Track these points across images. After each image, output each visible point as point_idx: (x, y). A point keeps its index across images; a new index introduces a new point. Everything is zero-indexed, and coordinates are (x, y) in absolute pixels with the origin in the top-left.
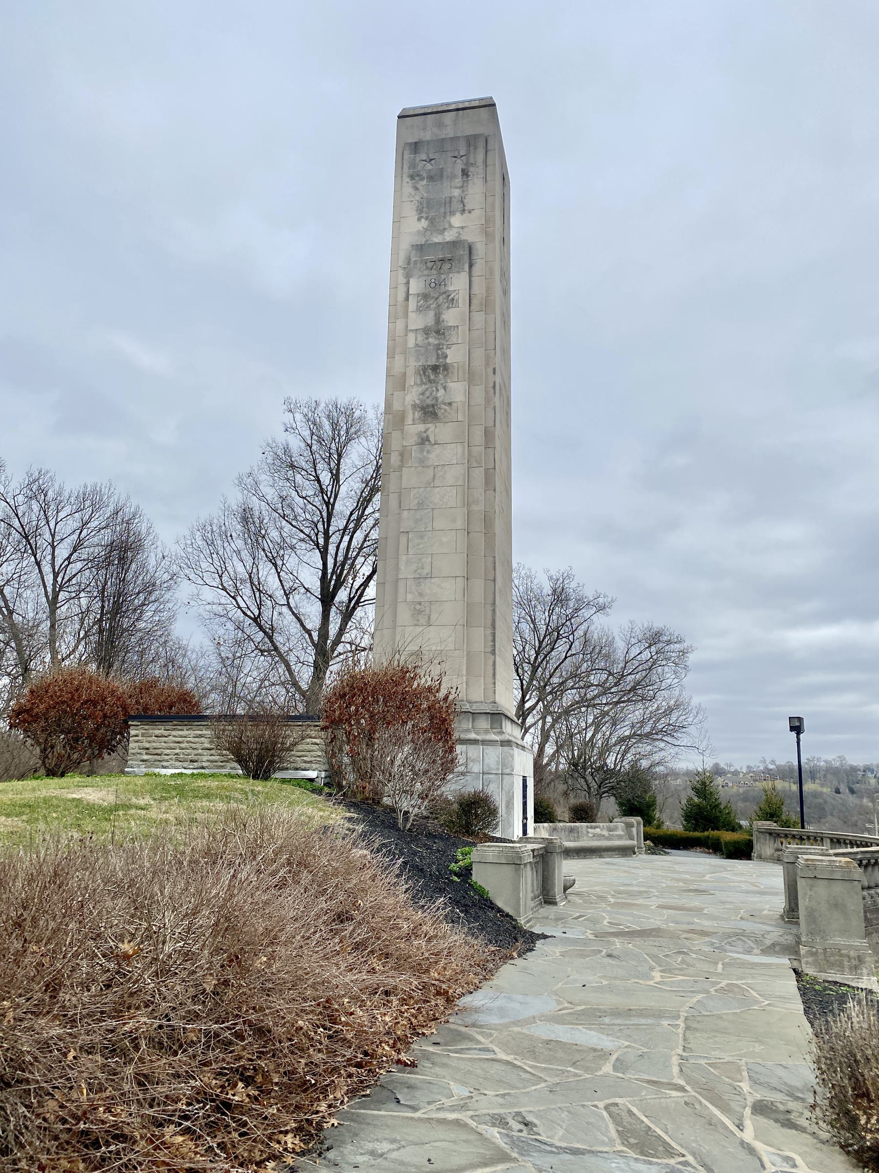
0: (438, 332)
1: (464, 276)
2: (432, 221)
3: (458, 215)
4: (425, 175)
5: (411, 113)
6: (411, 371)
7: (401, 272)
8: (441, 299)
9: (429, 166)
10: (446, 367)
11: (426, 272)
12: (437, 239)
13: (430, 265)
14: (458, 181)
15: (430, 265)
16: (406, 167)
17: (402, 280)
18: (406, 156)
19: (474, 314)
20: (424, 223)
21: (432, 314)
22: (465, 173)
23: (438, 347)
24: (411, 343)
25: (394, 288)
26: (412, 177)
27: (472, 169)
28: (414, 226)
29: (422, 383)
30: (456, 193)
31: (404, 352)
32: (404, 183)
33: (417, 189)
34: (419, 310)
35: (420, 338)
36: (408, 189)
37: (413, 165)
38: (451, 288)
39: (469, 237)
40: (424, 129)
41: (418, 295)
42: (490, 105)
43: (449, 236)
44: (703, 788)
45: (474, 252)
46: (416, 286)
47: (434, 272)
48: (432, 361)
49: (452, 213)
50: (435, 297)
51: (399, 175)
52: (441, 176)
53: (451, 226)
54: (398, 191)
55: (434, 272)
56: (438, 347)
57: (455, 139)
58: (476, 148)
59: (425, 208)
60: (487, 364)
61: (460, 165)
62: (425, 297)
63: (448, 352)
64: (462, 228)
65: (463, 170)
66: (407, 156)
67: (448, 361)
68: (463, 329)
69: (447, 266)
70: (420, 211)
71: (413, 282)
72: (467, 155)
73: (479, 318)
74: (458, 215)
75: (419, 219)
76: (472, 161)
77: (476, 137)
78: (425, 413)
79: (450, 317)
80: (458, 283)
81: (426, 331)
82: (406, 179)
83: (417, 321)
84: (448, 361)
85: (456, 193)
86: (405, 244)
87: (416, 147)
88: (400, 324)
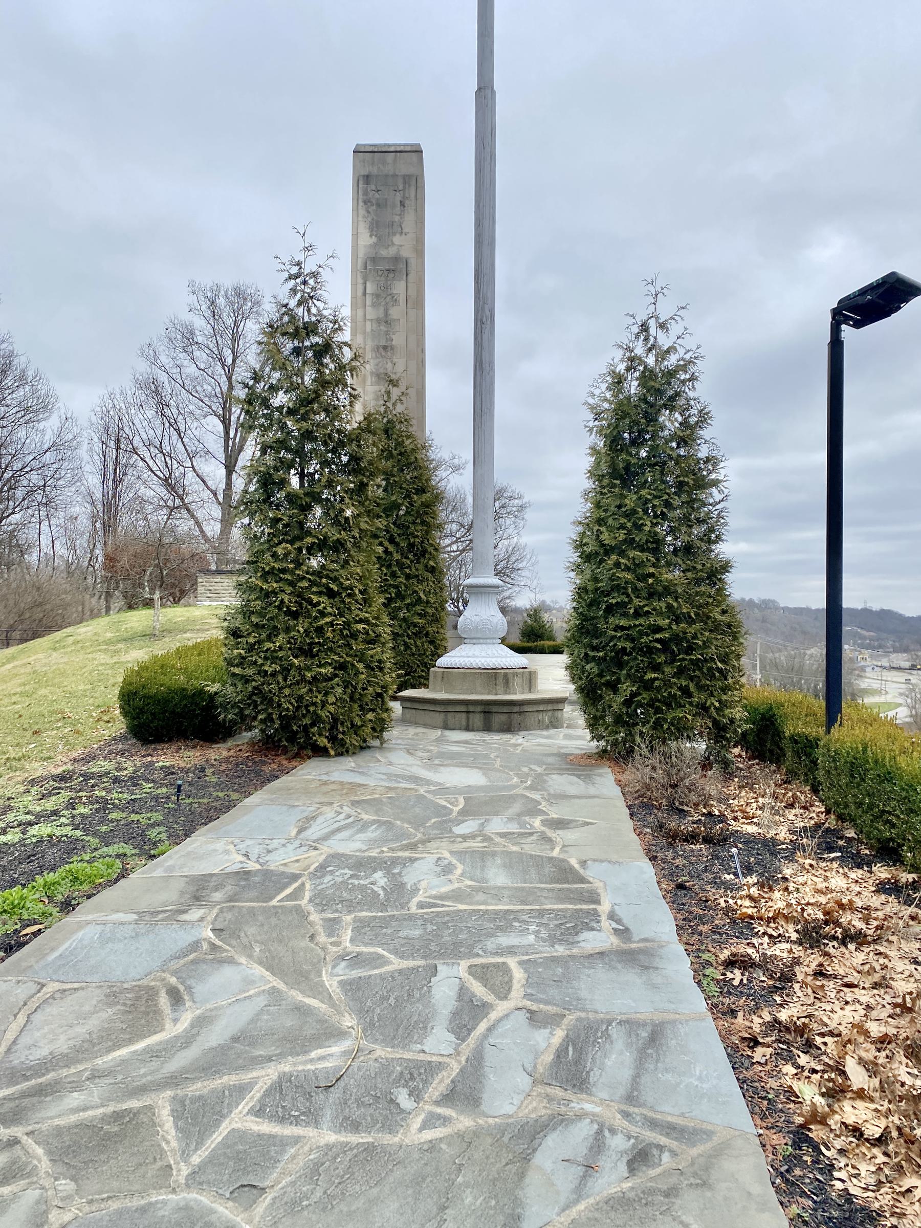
0: (386, 322)
1: (403, 283)
2: (380, 239)
3: (398, 235)
4: (374, 202)
5: (363, 150)
6: (368, 348)
7: (359, 274)
8: (388, 299)
9: (377, 196)
10: (392, 348)
11: (378, 278)
12: (384, 253)
13: (380, 273)
14: (398, 209)
15: (380, 273)
16: (361, 196)
17: (360, 281)
18: (361, 186)
19: (409, 310)
20: (374, 239)
21: (382, 309)
22: (402, 204)
23: (387, 333)
24: (368, 329)
25: (354, 285)
26: (365, 202)
27: (407, 202)
28: (366, 240)
29: (377, 357)
30: (397, 218)
31: (364, 333)
32: (360, 207)
33: (368, 212)
34: (373, 305)
35: (375, 326)
36: (362, 212)
37: (366, 193)
38: (395, 292)
39: (406, 253)
40: (373, 164)
41: (373, 294)
42: (418, 151)
43: (391, 252)
44: (535, 613)
45: (409, 265)
46: (370, 288)
47: (383, 278)
48: (383, 343)
49: (394, 234)
50: (384, 297)
51: (356, 199)
52: (386, 204)
53: (393, 244)
54: (356, 210)
55: (383, 278)
56: (387, 333)
57: (395, 176)
58: (410, 186)
59: (375, 227)
60: (418, 346)
61: (399, 197)
62: (377, 296)
63: (394, 337)
64: (401, 246)
65: (401, 202)
66: (361, 182)
67: (394, 343)
68: (403, 321)
69: (391, 275)
70: (371, 229)
71: (368, 285)
72: (404, 190)
73: (412, 313)
74: (398, 235)
75: (371, 236)
76: (407, 195)
77: (410, 176)
78: (379, 378)
79: (395, 312)
80: (399, 288)
81: (378, 321)
82: (361, 204)
83: (371, 313)
84: (394, 343)
85: (397, 218)
86: (361, 254)
87: (367, 178)
88: (360, 312)
